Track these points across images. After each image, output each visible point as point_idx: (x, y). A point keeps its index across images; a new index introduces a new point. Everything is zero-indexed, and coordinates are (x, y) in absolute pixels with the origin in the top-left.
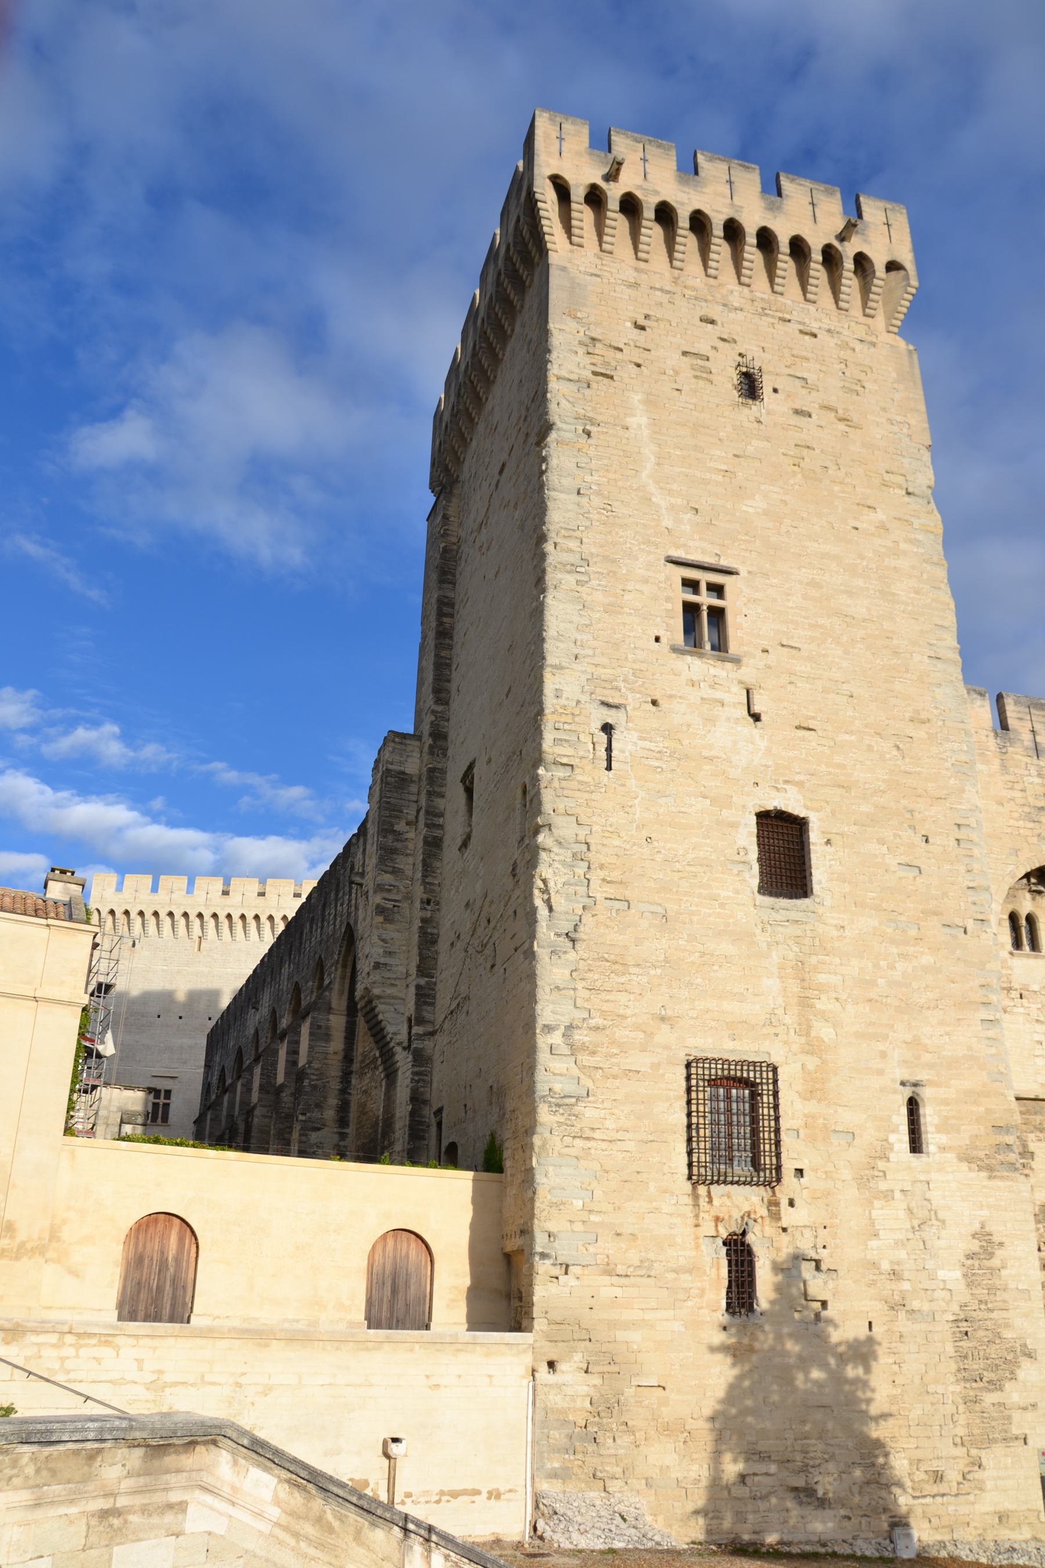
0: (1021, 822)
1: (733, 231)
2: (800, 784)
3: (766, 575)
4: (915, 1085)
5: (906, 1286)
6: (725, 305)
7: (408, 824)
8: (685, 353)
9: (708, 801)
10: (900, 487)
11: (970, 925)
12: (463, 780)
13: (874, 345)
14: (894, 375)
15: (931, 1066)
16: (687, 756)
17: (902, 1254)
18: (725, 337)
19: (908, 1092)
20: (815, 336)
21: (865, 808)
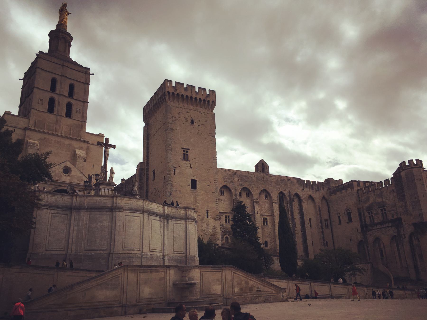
0: (222, 180)
1: (191, 97)
2: (196, 176)
3: (193, 149)
4: (208, 210)
5: (206, 232)
6: (190, 109)
7: (143, 175)
8: (184, 118)
9: (185, 178)
10: (211, 136)
11: (215, 192)
12: (153, 171)
13: (209, 114)
14: (212, 119)
15: (209, 208)
16: (183, 173)
17: (205, 228)
18: (190, 115)
19: (207, 211)
20: (201, 113)
21: (204, 179)
